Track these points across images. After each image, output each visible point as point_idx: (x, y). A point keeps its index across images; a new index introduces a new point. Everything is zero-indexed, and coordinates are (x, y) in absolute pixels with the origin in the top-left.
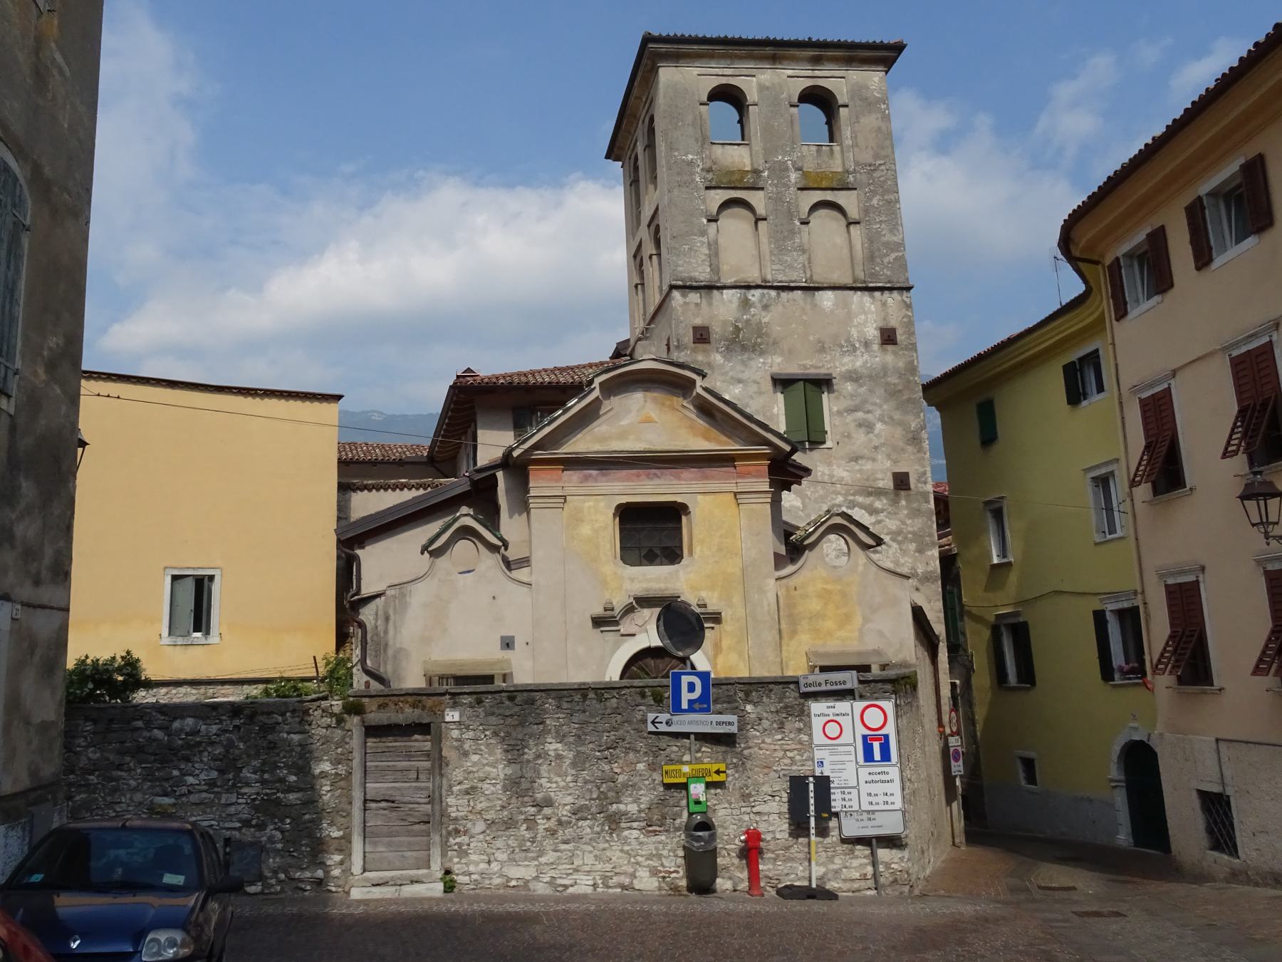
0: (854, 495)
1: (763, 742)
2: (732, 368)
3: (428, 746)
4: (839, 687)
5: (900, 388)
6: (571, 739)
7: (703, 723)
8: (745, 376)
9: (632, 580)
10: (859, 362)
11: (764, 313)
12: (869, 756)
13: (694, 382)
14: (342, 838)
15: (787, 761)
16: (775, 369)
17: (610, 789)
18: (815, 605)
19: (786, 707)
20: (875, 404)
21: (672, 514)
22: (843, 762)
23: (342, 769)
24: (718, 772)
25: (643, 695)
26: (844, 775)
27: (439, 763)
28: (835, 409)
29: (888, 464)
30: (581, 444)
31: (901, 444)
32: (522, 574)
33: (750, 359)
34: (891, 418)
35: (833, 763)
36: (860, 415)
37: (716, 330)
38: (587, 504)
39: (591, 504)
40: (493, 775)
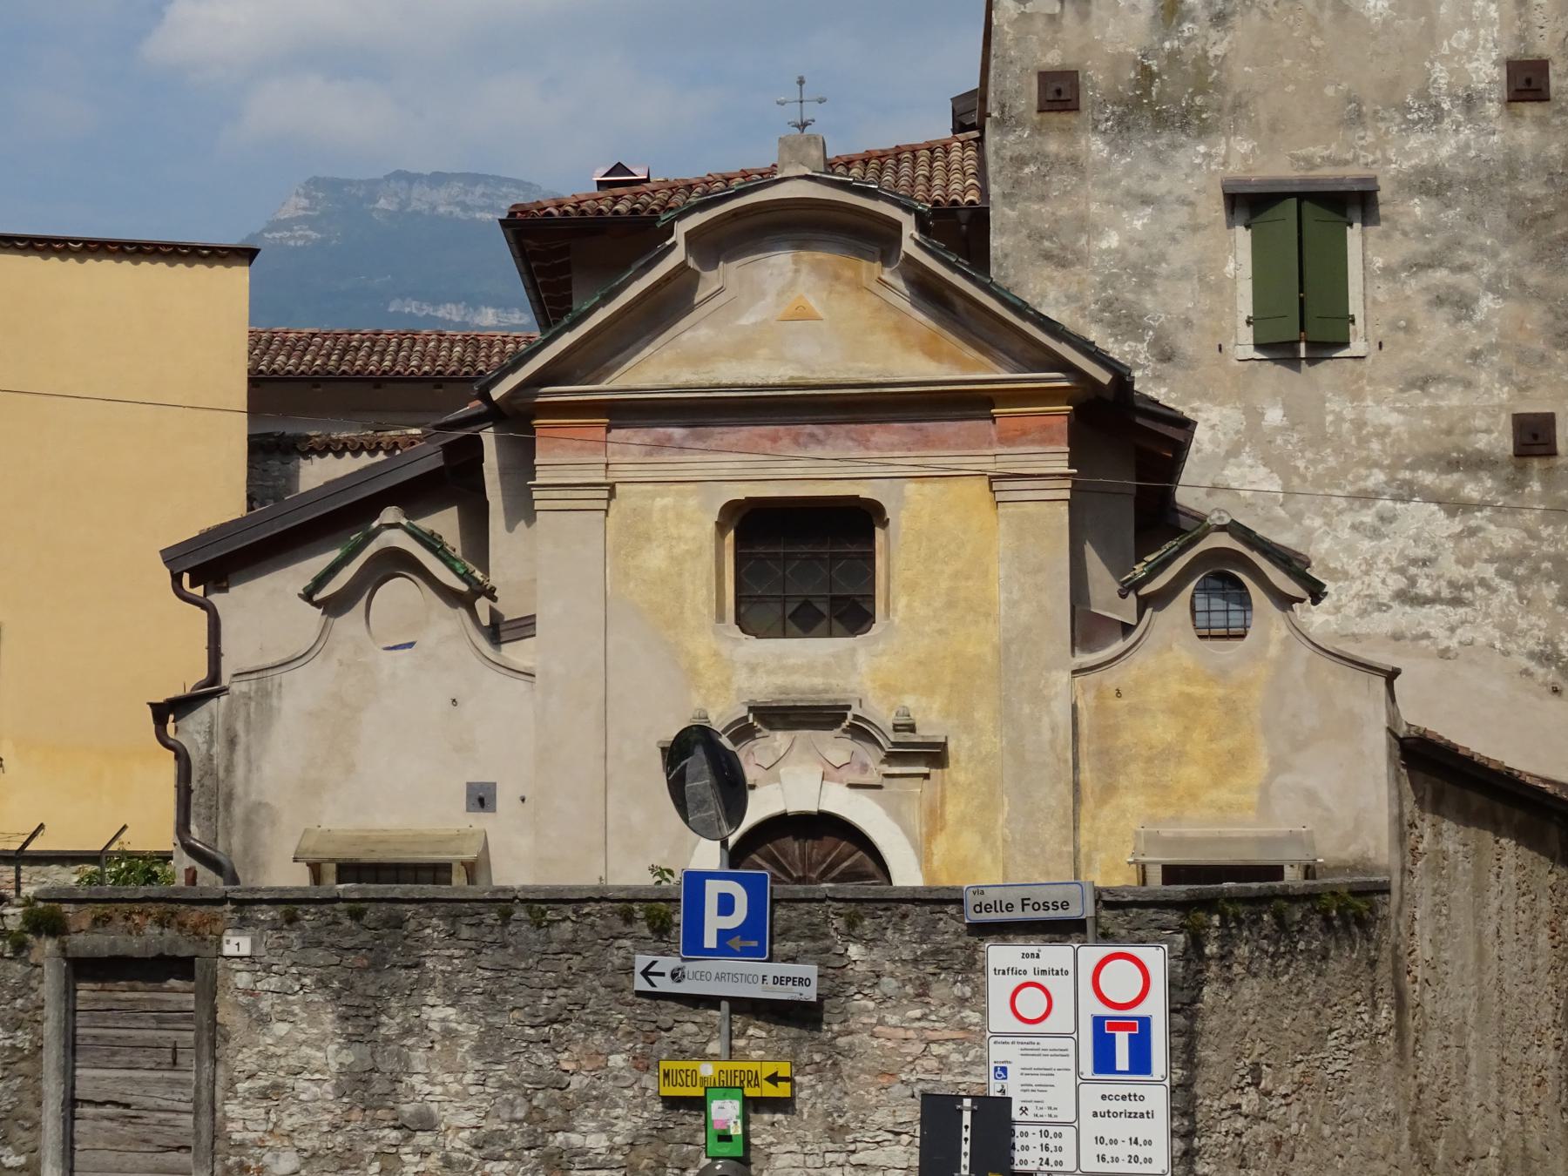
0: (1413, 467)
1: (881, 1022)
2: (1128, 172)
3: (189, 1001)
4: (1052, 914)
5: (1548, 208)
6: (476, 1000)
7: (746, 978)
8: (1159, 187)
9: (753, 669)
10: (1447, 147)
11: (1213, 34)
12: (1104, 1061)
13: (898, 226)
14: (22, 1169)
15: (933, 1064)
16: (1236, 170)
17: (552, 1103)
18: (1161, 731)
19: (936, 952)
20: (1481, 249)
21: (852, 524)
22: (1049, 1072)
23: (23, 1039)
24: (774, 1079)
25: (628, 918)
26: (1049, 1098)
27: (212, 1036)
28: (1379, 262)
29: (1504, 394)
30: (651, 370)
31: (1539, 345)
32: (516, 653)
33: (1173, 146)
34: (1520, 283)
35: (1026, 1072)
36: (1441, 275)
37: (1096, 80)
38: (659, 502)
39: (668, 501)
40: (316, 1064)
